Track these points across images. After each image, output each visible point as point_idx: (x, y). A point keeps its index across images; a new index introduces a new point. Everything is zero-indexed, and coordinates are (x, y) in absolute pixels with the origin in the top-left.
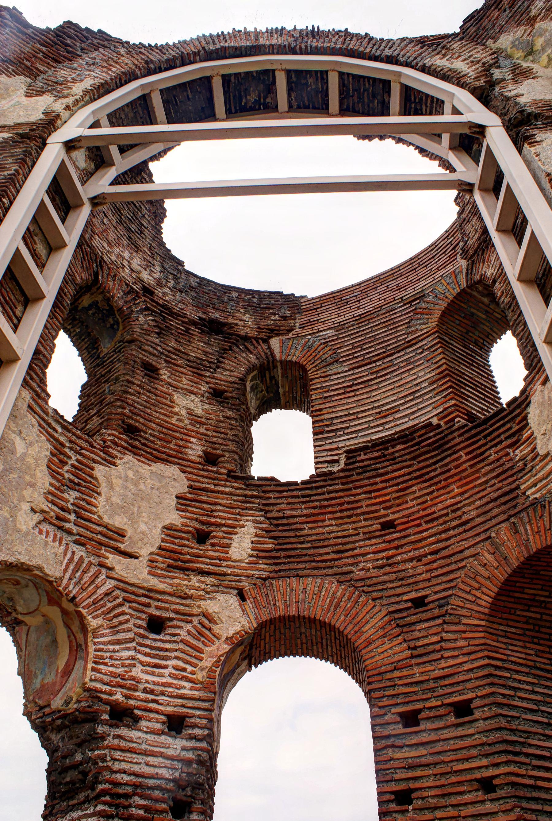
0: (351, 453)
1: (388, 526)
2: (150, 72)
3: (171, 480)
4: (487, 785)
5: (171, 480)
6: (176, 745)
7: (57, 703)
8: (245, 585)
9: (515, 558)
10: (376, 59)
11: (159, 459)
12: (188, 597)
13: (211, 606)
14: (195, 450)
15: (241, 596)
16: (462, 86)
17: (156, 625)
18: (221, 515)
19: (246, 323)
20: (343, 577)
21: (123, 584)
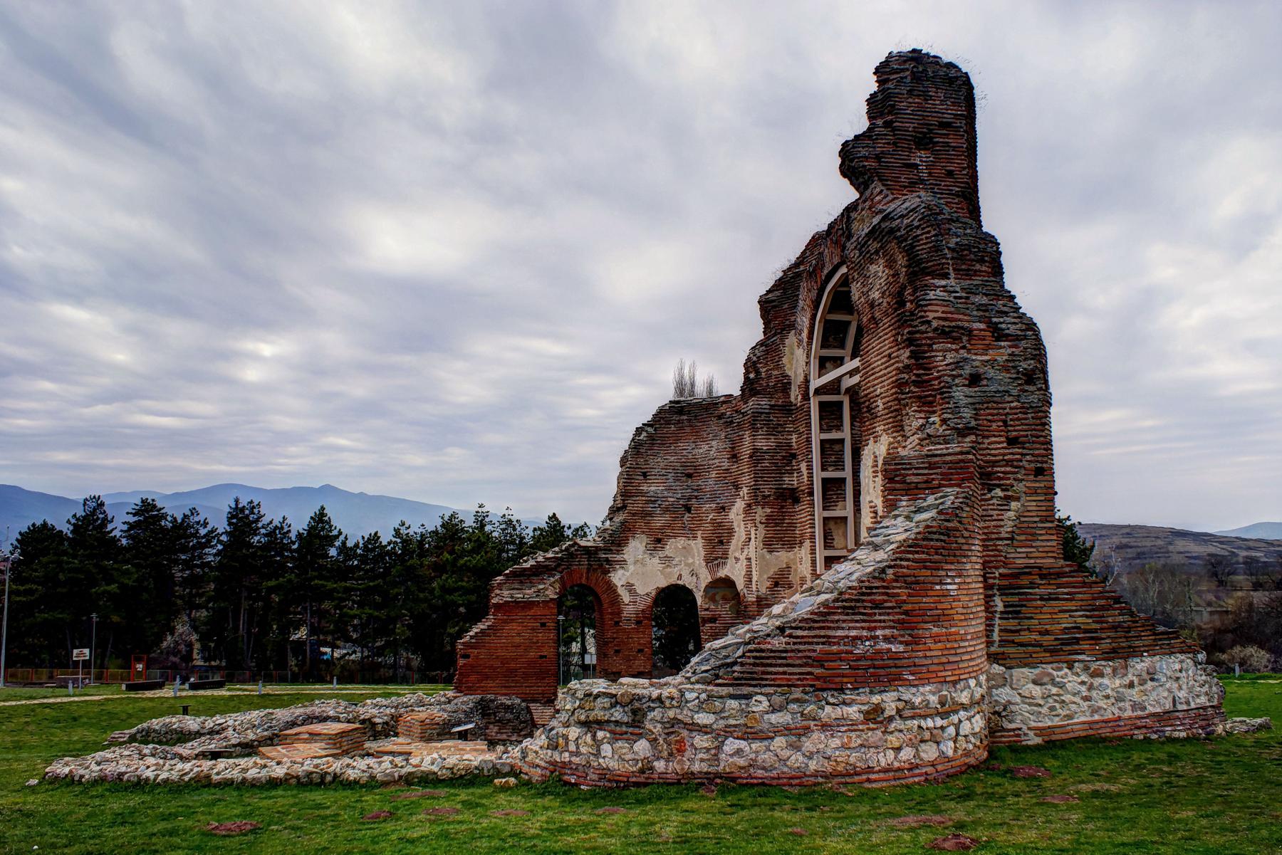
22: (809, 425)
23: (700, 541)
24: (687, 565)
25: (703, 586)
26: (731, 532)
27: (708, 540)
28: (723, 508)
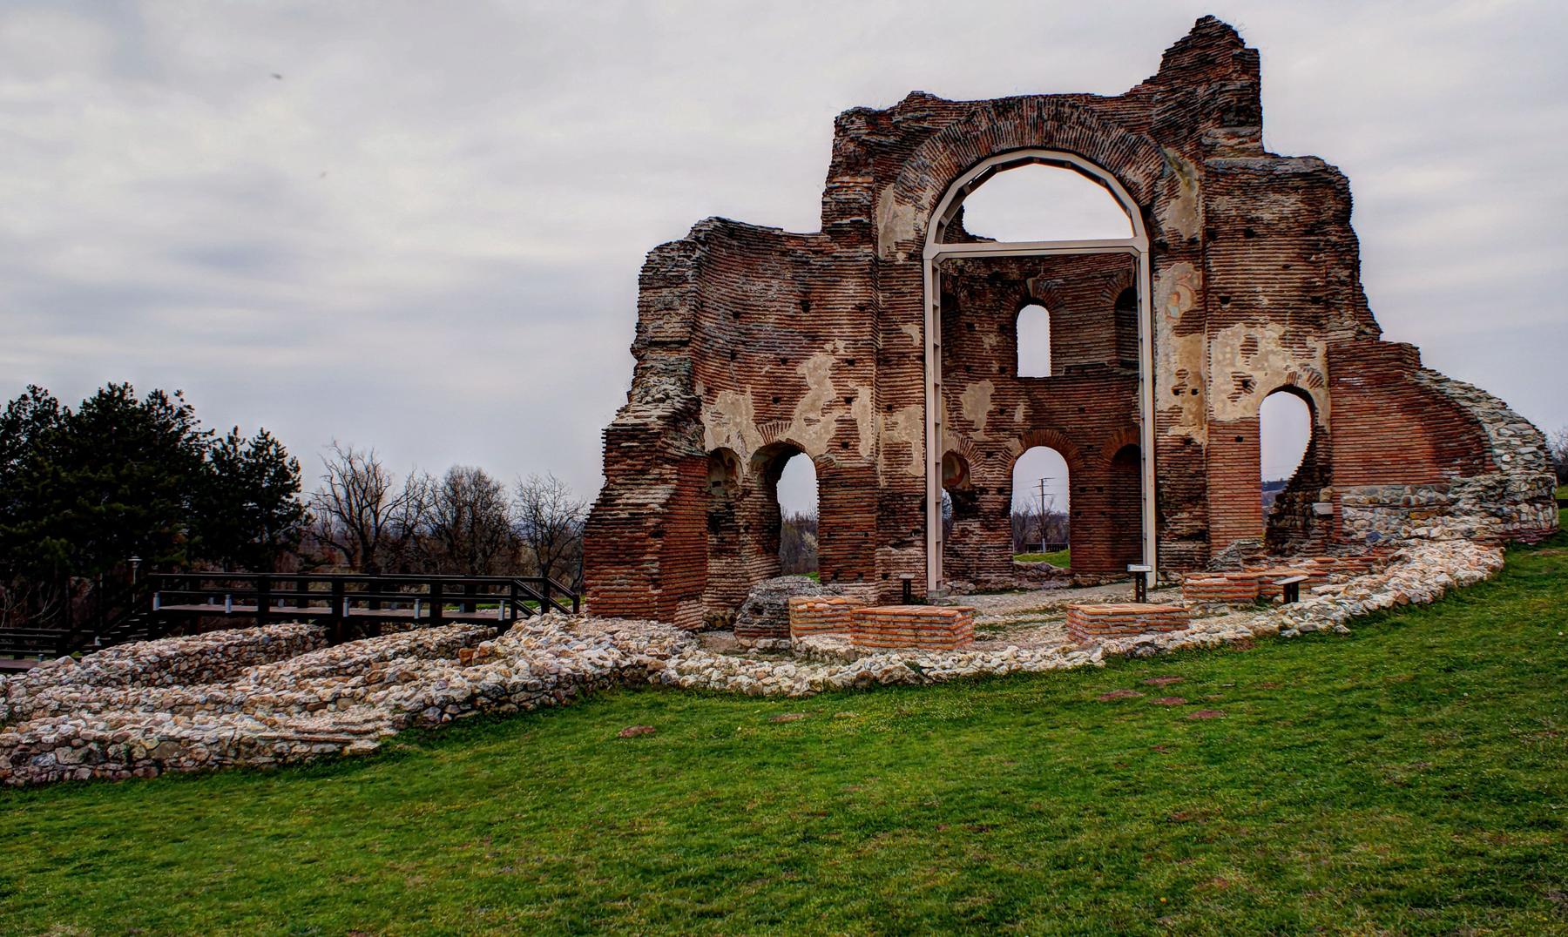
0: (1069, 369)
1: (1082, 410)
2: (961, 174)
3: (988, 386)
5: (988, 386)
6: (1001, 498)
7: (959, 487)
11: (981, 379)
14: (995, 367)
15: (1020, 437)
16: (1137, 201)
17: (989, 455)
18: (1010, 400)
19: (1014, 272)
20: (1062, 431)
21: (977, 443)
22: (922, 286)
23: (749, 396)
24: (736, 424)
25: (752, 450)
26: (799, 389)
27: (760, 397)
28: (784, 361)
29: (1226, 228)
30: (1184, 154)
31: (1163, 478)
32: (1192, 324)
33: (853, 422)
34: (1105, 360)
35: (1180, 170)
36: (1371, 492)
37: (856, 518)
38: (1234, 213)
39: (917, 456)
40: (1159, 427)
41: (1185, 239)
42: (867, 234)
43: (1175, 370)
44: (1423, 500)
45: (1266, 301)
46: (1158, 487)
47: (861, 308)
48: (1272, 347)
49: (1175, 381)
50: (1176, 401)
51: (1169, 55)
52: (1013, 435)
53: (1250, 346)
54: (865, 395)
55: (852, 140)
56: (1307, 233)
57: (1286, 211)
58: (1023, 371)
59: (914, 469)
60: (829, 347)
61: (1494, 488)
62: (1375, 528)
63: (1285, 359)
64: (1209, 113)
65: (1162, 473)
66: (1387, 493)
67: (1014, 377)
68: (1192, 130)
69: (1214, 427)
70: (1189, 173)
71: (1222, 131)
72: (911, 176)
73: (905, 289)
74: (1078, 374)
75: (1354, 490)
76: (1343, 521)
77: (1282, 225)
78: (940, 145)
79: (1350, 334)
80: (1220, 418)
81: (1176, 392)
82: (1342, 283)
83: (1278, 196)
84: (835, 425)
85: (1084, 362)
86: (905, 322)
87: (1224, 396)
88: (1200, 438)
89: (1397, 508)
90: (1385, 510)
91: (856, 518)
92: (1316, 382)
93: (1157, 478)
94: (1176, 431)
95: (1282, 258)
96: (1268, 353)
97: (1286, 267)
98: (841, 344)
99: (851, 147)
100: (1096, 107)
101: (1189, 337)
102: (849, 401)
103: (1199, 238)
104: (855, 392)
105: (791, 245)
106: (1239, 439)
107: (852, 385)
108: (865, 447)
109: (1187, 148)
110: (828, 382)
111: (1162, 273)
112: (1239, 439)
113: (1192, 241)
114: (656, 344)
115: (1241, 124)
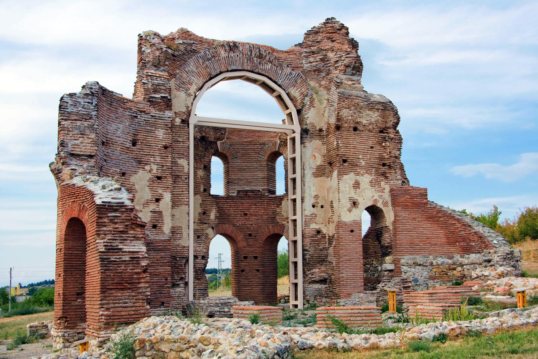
0: (239, 192)
1: (246, 214)
4: (258, 270)
6: (204, 261)
8: (214, 226)
9: (272, 233)
10: (276, 83)
12: (203, 230)
13: (207, 231)
14: (202, 190)
15: (213, 228)
16: (295, 106)
19: (212, 136)
20: (234, 225)
28: (124, 174)
29: (346, 125)
30: (321, 86)
31: (306, 250)
32: (320, 172)
33: (160, 213)
34: (260, 188)
35: (317, 93)
36: (413, 259)
37: (161, 270)
38: (350, 118)
39: (185, 234)
40: (306, 224)
41: (317, 129)
42: (167, 103)
43: (313, 195)
44: (440, 263)
45: (363, 163)
46: (304, 255)
47: (166, 147)
48: (368, 186)
49: (313, 201)
50: (314, 210)
51: (308, 34)
52: (208, 227)
53: (357, 185)
54: (167, 197)
55: (158, 49)
56: (381, 132)
57: (373, 120)
58: (213, 192)
59: (182, 243)
60: (147, 168)
61: (508, 254)
62: (416, 276)
63: (372, 192)
64: (338, 67)
65: (307, 248)
66: (422, 259)
67: (210, 193)
68: (328, 74)
69: (340, 225)
70: (321, 96)
71: (345, 77)
72: (185, 75)
73: (180, 139)
74: (244, 194)
75: (407, 257)
76: (401, 273)
77: (371, 127)
78: (201, 61)
79: (400, 182)
80: (344, 220)
81: (313, 206)
82: (396, 157)
83: (370, 112)
84: (150, 214)
85: (248, 188)
86: (180, 158)
87: (346, 209)
88: (329, 230)
89: (426, 266)
90: (421, 267)
91: (161, 270)
92: (385, 204)
93: (304, 250)
94: (314, 226)
95: (370, 143)
96: (365, 189)
97: (372, 147)
98: (155, 167)
99: (158, 53)
100: (275, 54)
101: (320, 178)
102: (158, 200)
103: (324, 129)
104: (161, 195)
105: (129, 105)
106: (352, 231)
107: (160, 191)
108: (167, 228)
109: (323, 83)
110: (147, 189)
111: (307, 144)
112: (352, 231)
113: (321, 130)
114: (72, 155)
115: (353, 75)
